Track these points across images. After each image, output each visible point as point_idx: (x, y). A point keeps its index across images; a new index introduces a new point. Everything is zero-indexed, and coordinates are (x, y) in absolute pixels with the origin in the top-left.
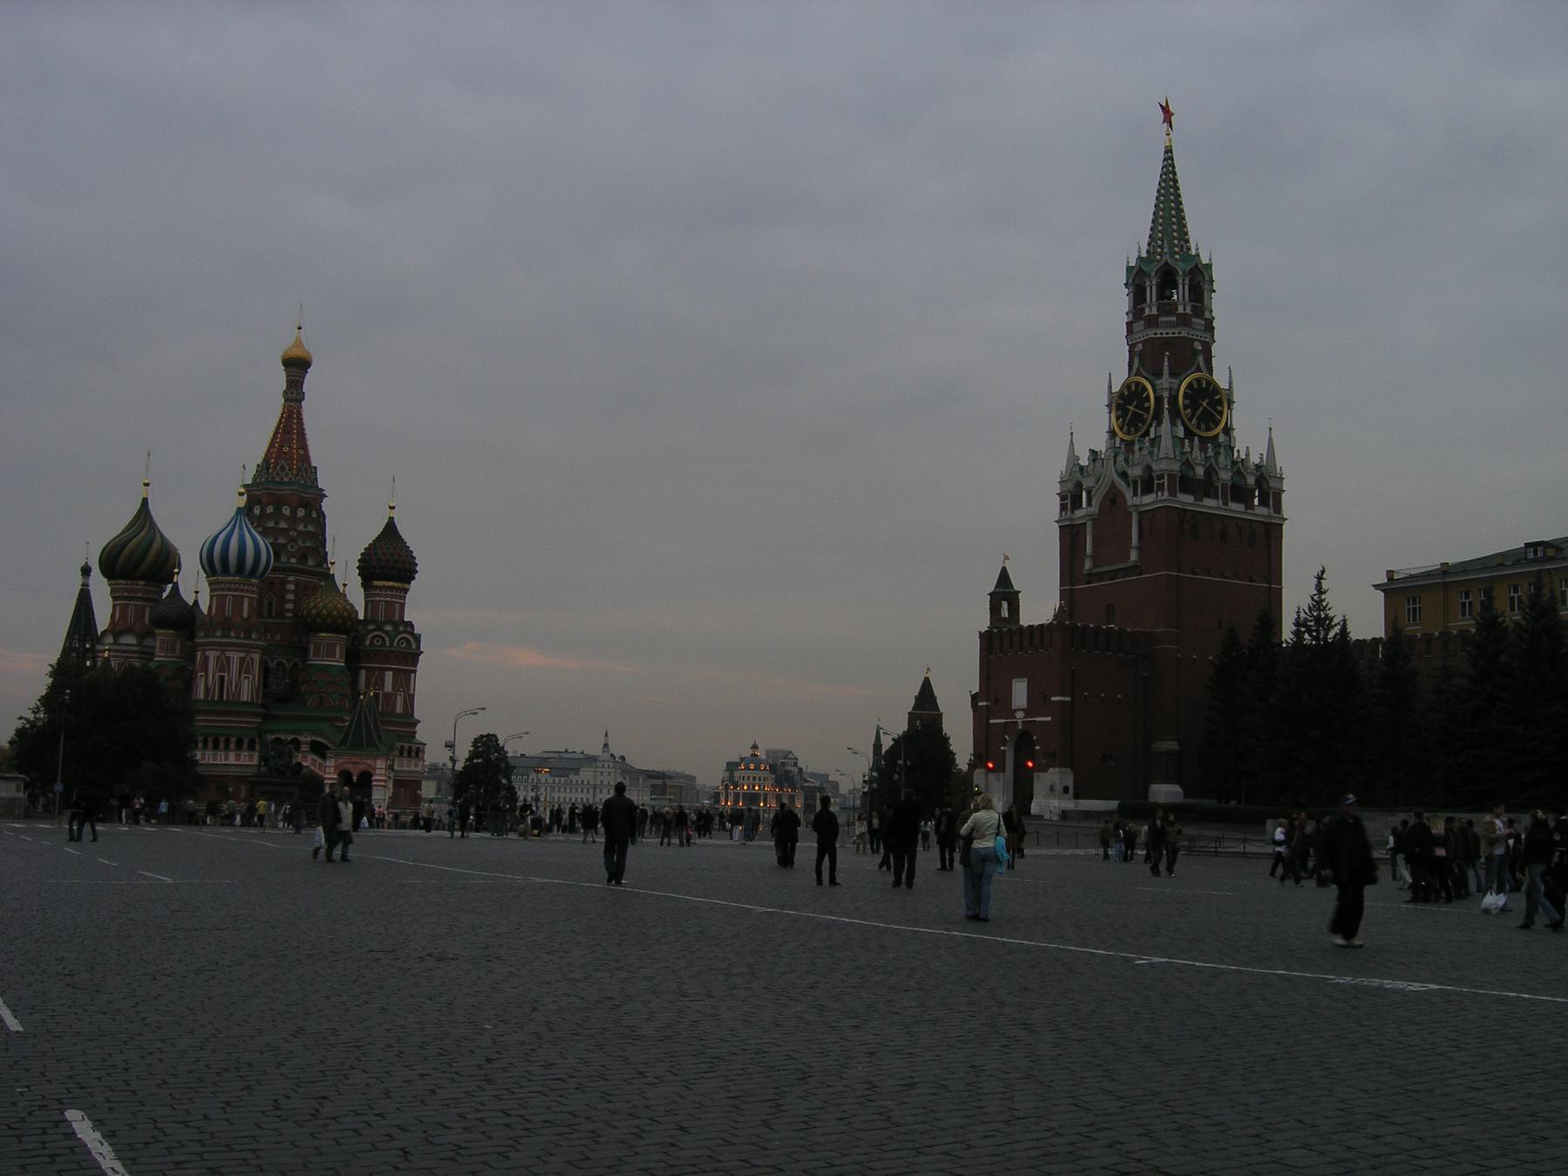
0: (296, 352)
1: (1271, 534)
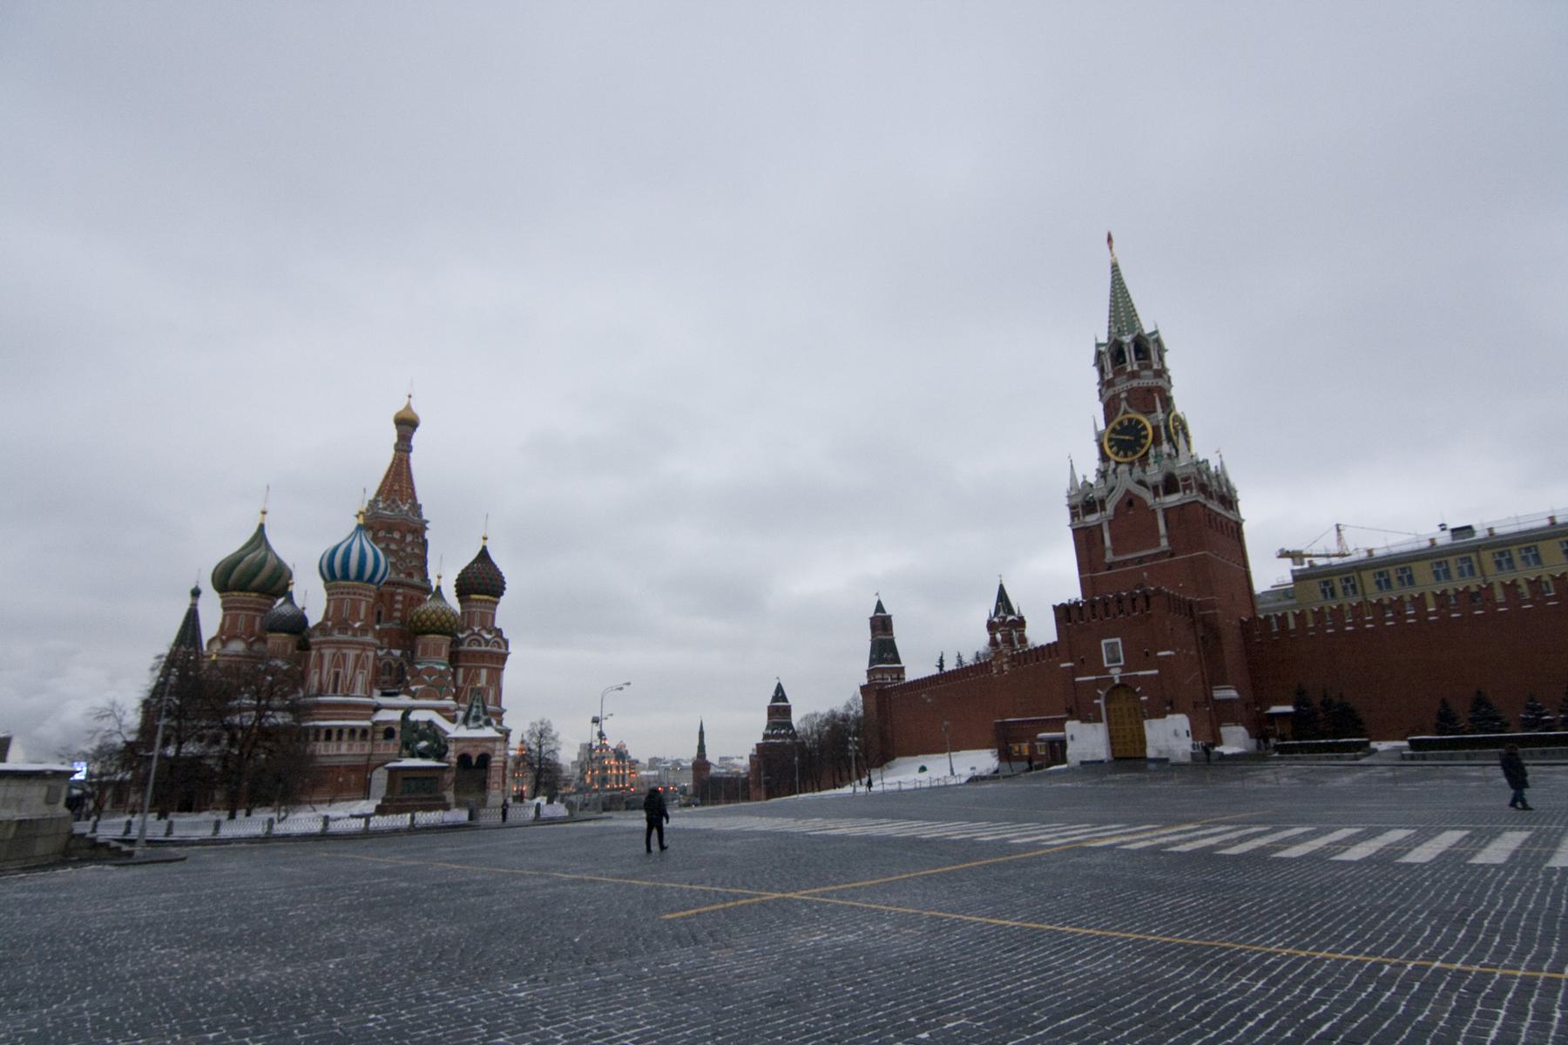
0: (405, 416)
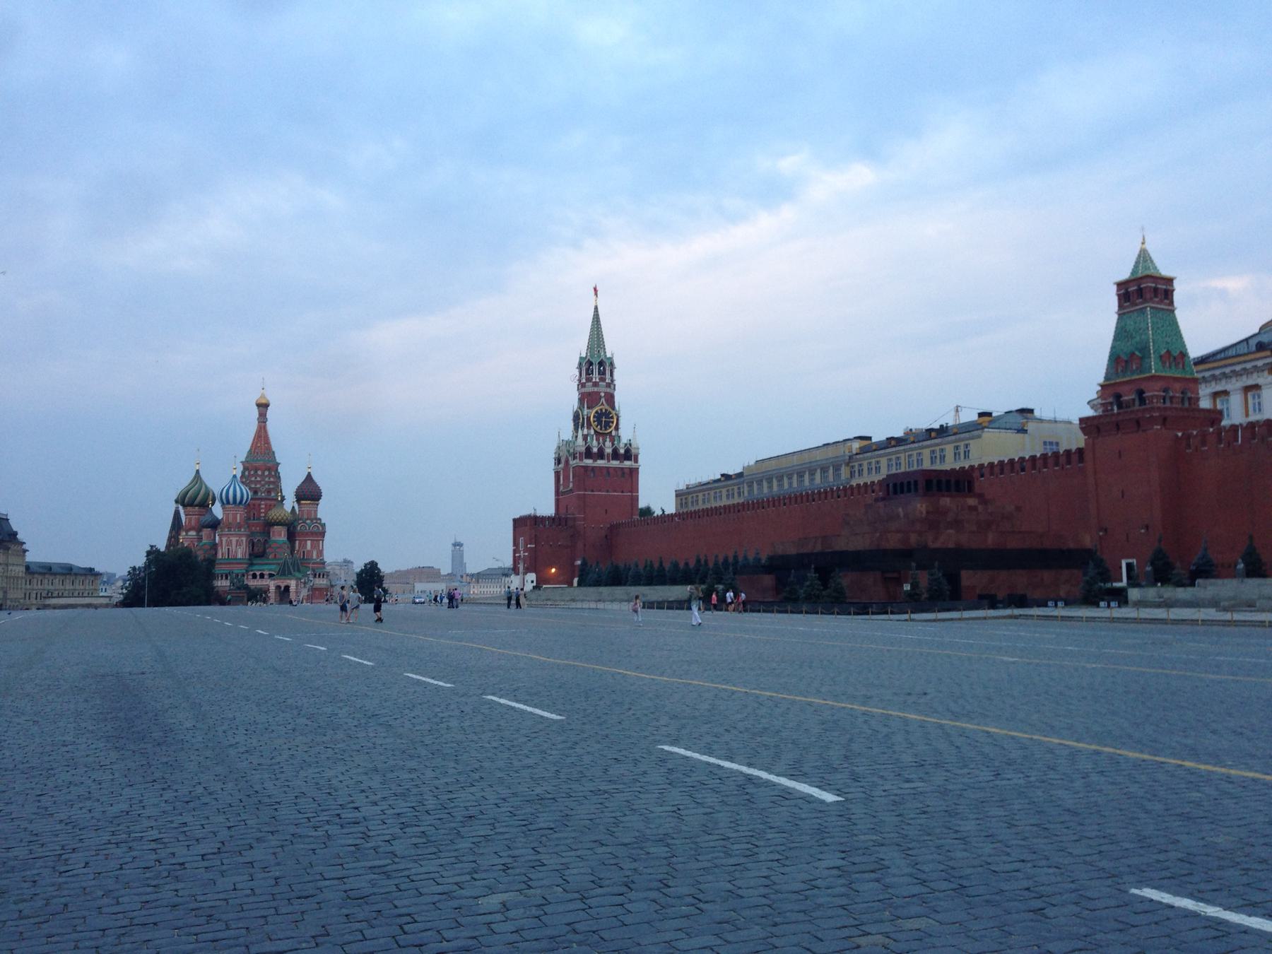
0: (264, 401)
1: (633, 473)
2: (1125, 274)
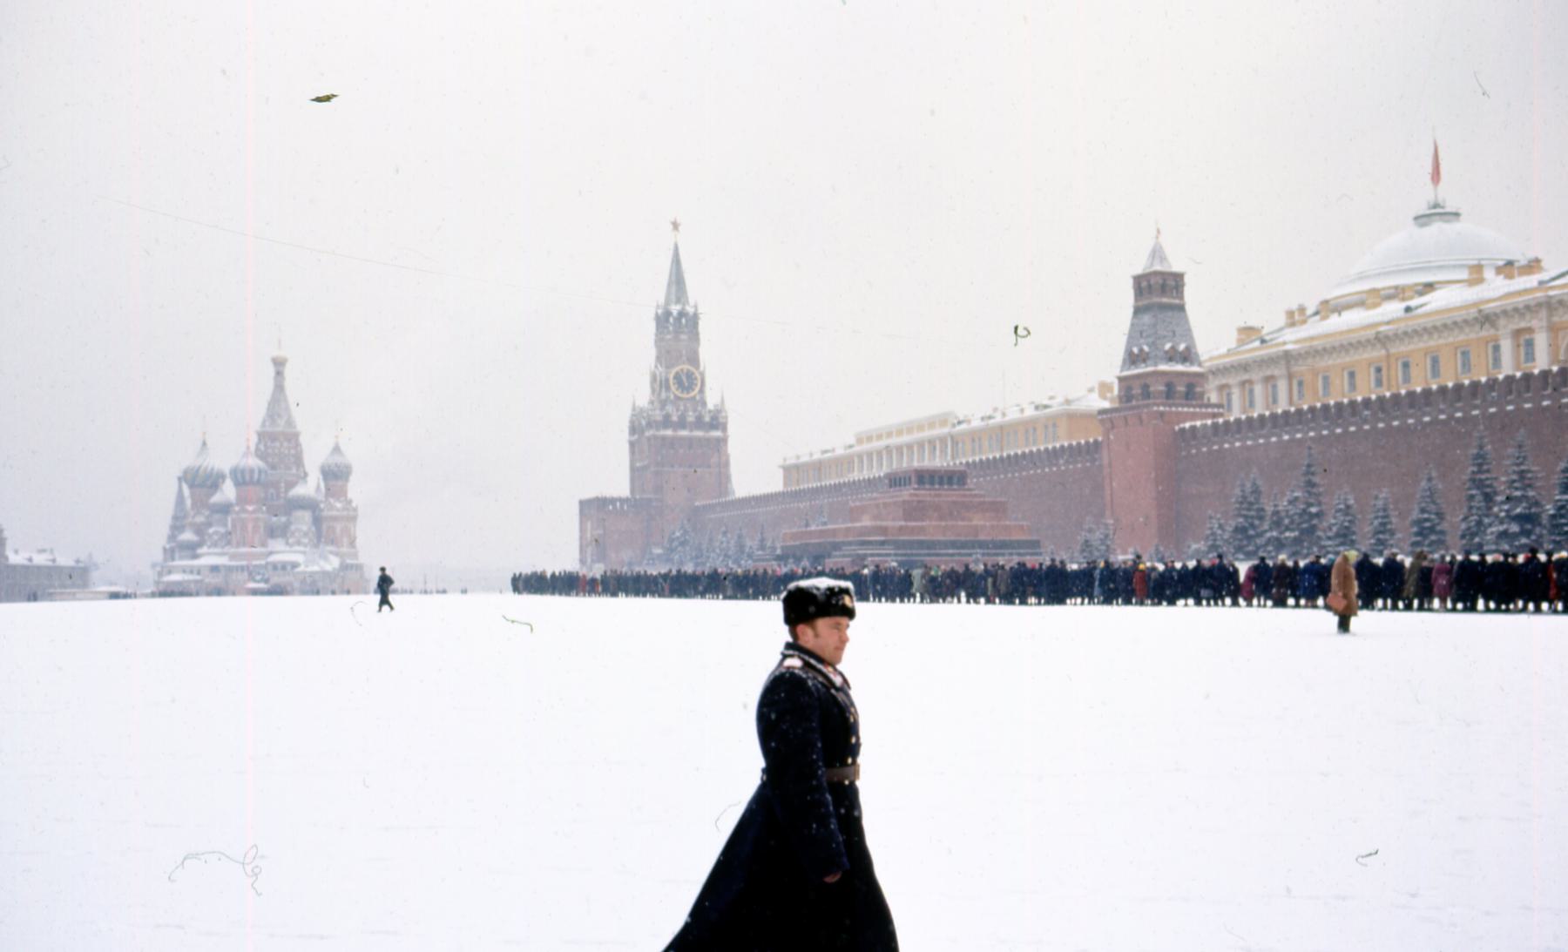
2: (1139, 271)
